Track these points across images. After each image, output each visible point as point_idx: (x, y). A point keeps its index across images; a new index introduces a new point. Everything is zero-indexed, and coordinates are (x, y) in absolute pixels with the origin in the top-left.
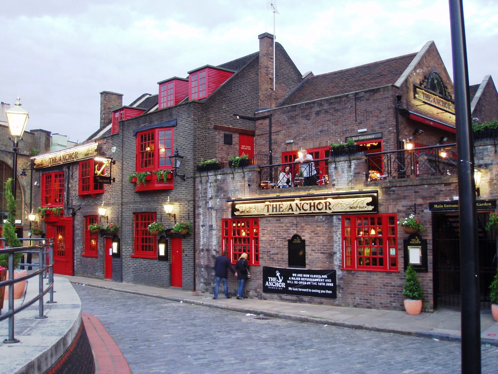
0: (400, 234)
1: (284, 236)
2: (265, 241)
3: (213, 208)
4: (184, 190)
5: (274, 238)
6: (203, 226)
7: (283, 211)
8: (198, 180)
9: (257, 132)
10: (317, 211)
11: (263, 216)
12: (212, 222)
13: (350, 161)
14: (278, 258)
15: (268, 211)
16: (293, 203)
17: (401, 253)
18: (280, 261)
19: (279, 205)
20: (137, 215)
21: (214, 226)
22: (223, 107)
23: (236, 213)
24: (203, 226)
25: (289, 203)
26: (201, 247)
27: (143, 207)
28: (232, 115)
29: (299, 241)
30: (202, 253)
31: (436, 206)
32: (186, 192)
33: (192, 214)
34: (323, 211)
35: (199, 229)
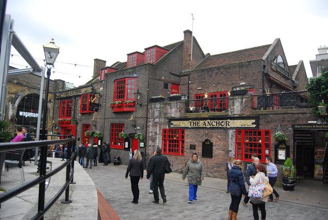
0: (273, 141)
1: (200, 140)
8: (149, 107)
10: (221, 126)
13: (242, 98)
16: (206, 122)
17: (273, 153)
20: (113, 125)
21: (158, 132)
23: (172, 126)
27: (117, 121)
29: (209, 143)
31: (296, 126)
33: (145, 125)
34: (225, 126)
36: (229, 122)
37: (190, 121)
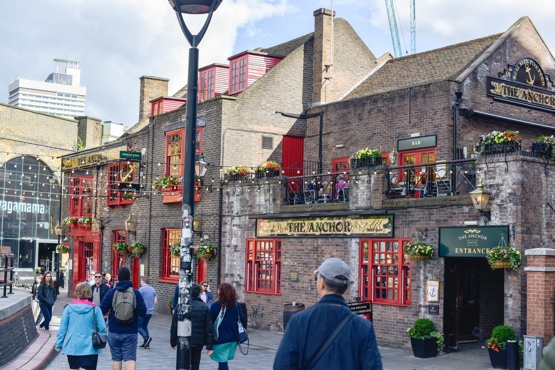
2: (287, 265)
4: (211, 203)
5: (296, 263)
7: (304, 231)
9: (308, 133)
11: (285, 236)
14: (298, 287)
15: (290, 231)
16: (315, 222)
18: (301, 290)
19: (301, 224)
22: (263, 103)
24: (228, 246)
25: (311, 222)
26: (226, 272)
28: (274, 112)
32: (212, 206)
35: (225, 251)
36: (349, 225)
37: (290, 221)
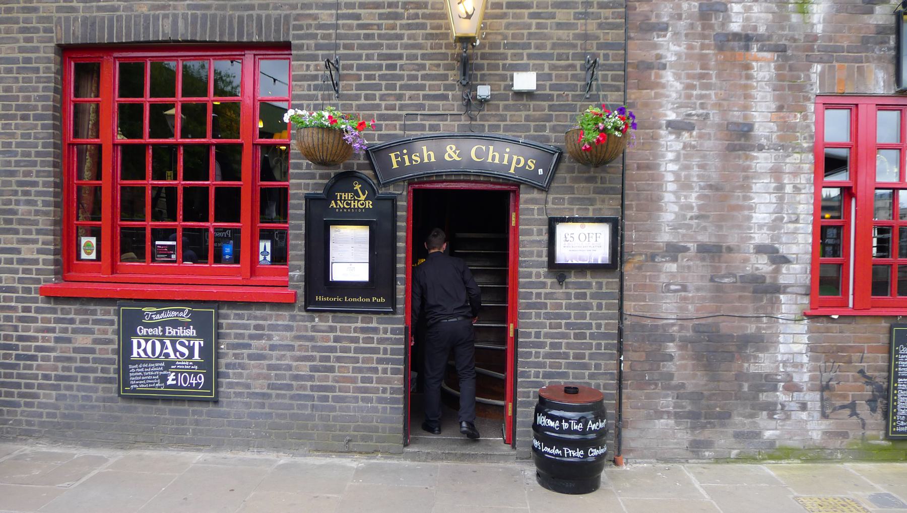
3: (759, 38)
6: (676, 127)
12: (746, 108)
26: (665, 237)
30: (673, 267)
